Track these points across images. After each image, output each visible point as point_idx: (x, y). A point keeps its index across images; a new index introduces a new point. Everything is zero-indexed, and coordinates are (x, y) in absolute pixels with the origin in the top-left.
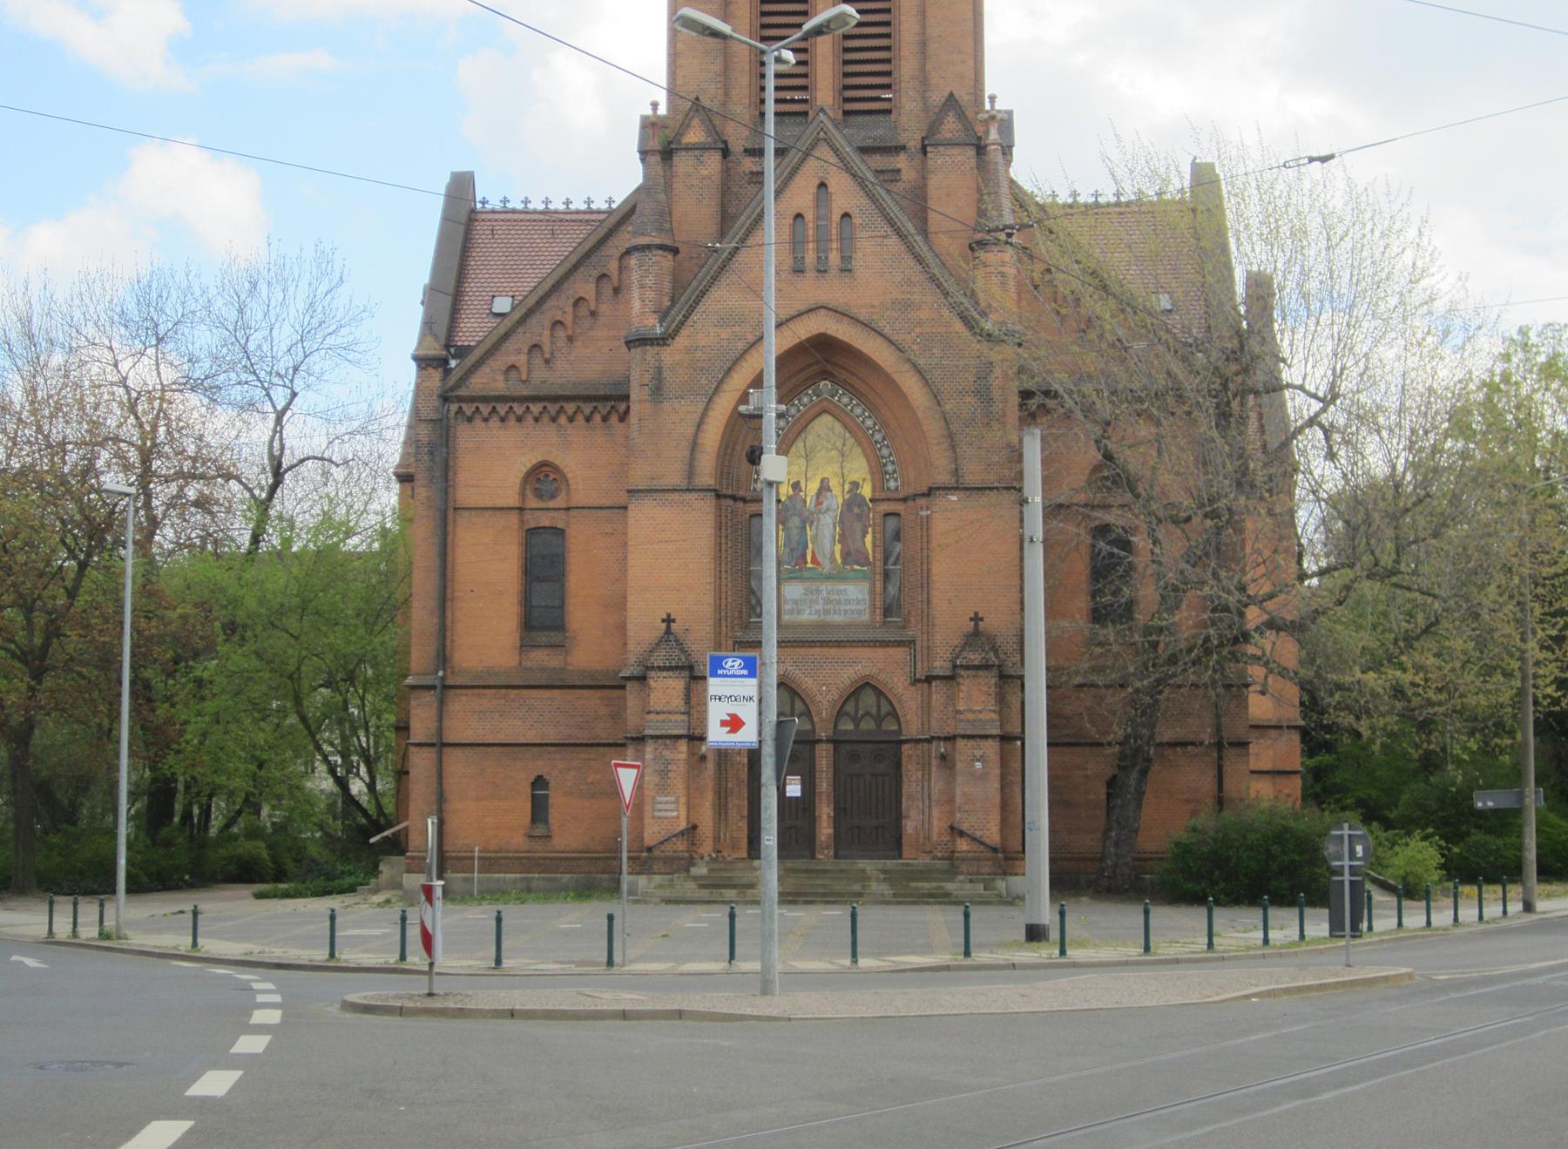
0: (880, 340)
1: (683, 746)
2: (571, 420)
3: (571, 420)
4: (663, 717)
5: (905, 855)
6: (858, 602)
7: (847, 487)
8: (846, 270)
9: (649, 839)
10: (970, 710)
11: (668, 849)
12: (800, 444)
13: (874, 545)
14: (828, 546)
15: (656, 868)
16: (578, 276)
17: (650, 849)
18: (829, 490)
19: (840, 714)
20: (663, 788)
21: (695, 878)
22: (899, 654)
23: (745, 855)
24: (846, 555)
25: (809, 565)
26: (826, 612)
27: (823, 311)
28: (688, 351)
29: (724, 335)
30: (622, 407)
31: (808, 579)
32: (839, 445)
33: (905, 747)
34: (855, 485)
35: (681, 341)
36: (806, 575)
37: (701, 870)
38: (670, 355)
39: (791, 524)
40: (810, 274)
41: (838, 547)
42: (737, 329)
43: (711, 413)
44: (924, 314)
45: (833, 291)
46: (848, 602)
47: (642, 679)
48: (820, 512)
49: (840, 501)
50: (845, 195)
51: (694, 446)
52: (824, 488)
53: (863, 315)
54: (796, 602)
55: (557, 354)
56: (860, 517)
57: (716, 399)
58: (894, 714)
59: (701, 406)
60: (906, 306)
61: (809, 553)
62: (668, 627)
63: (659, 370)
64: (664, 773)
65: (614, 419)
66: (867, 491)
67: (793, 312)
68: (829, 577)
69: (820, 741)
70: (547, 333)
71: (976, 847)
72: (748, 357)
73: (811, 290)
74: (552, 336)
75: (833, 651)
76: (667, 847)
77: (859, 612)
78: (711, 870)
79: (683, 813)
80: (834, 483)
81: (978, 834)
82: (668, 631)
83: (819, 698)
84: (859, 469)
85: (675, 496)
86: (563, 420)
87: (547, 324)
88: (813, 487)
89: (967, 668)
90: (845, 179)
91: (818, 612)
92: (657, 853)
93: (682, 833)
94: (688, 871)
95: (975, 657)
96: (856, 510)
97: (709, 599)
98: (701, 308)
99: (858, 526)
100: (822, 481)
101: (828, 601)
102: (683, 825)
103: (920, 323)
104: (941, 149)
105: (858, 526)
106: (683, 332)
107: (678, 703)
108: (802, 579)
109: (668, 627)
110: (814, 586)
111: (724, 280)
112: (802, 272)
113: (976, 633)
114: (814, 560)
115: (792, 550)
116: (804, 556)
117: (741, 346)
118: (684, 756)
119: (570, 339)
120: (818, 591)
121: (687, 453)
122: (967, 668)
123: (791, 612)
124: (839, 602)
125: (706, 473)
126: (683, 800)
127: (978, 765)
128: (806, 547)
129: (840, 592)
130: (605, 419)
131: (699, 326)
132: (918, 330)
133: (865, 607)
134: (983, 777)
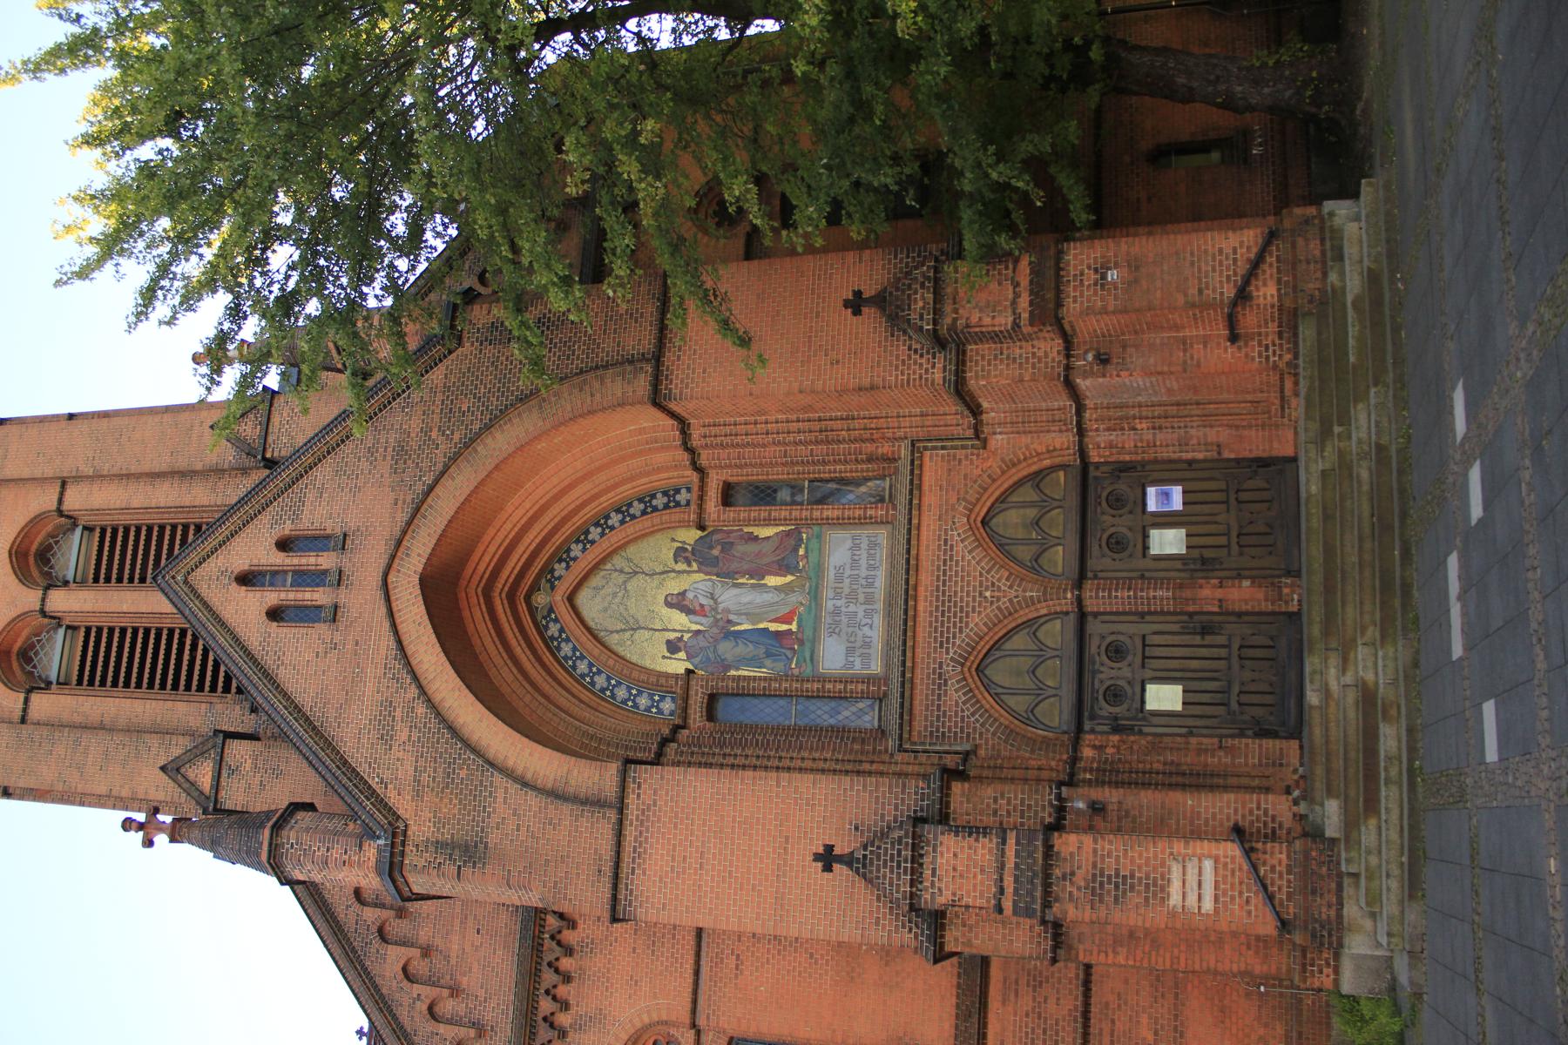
0: (438, 490)
1: (1067, 843)
2: (565, 1006)
3: (565, 1006)
4: (1009, 882)
5: (1289, 452)
6: (855, 547)
7: (682, 566)
8: (341, 542)
9: (1268, 927)
10: (1014, 303)
11: (1282, 885)
12: (612, 641)
13: (768, 522)
14: (769, 597)
15: (1327, 913)
16: (375, 970)
17: (1284, 925)
18: (683, 594)
19: (1035, 567)
20: (1157, 888)
21: (1351, 824)
22: (933, 467)
23: (1295, 744)
24: (783, 568)
25: (794, 627)
26: (869, 600)
27: (391, 578)
28: (418, 795)
29: (404, 736)
30: (552, 921)
31: (816, 630)
32: (622, 578)
33: (1094, 456)
34: (680, 554)
35: (403, 805)
36: (808, 633)
37: (1331, 814)
38: (420, 827)
39: (729, 657)
40: (343, 596)
41: (772, 581)
42: (398, 713)
43: (510, 763)
44: (415, 424)
45: (366, 563)
46: (855, 563)
47: (937, 920)
48: (715, 609)
49: (701, 576)
50: (255, 547)
51: (556, 794)
52: (678, 602)
53: (401, 518)
54: (850, 651)
55: (475, 1016)
56: (727, 547)
57: (491, 754)
58: (1037, 478)
59: (498, 778)
60: (401, 452)
61: (773, 627)
62: (840, 859)
63: (440, 845)
64: (1122, 884)
65: (569, 936)
66: (691, 536)
67: (387, 624)
68: (815, 595)
69: (1079, 601)
70: (442, 1029)
71: (1269, 269)
72: (437, 698)
73: (361, 599)
74: (450, 1022)
75: (926, 579)
76: (1282, 885)
77: (873, 545)
78: (1330, 793)
79: (1205, 847)
80: (674, 586)
81: (1243, 267)
82: (848, 860)
83: (1004, 603)
84: (658, 550)
85: (630, 833)
86: (563, 1019)
87: (431, 1026)
88: (679, 620)
89: (937, 312)
90: (238, 544)
91: (868, 613)
92: (1291, 910)
93: (1248, 852)
94: (1333, 841)
95: (921, 300)
96: (716, 552)
97: (804, 782)
98: (363, 770)
99: (741, 548)
100: (669, 604)
101: (852, 597)
102: (1233, 850)
103: (426, 431)
104: (270, 439)
105: (741, 548)
106: (392, 798)
107: (983, 850)
108: (815, 641)
109: (840, 859)
110: (826, 619)
111: (331, 731)
112: (336, 607)
113: (880, 301)
114: (786, 619)
115: (768, 655)
116: (777, 633)
117: (421, 709)
118: (1087, 840)
119: (455, 991)
120: (836, 612)
121: (566, 808)
122: (937, 312)
123: (866, 657)
124: (854, 579)
125: (598, 777)
126: (1178, 846)
127: (1112, 275)
128: (766, 630)
129: (839, 578)
130: (569, 951)
131: (387, 775)
132: (434, 435)
133: (864, 533)
134: (1134, 265)
